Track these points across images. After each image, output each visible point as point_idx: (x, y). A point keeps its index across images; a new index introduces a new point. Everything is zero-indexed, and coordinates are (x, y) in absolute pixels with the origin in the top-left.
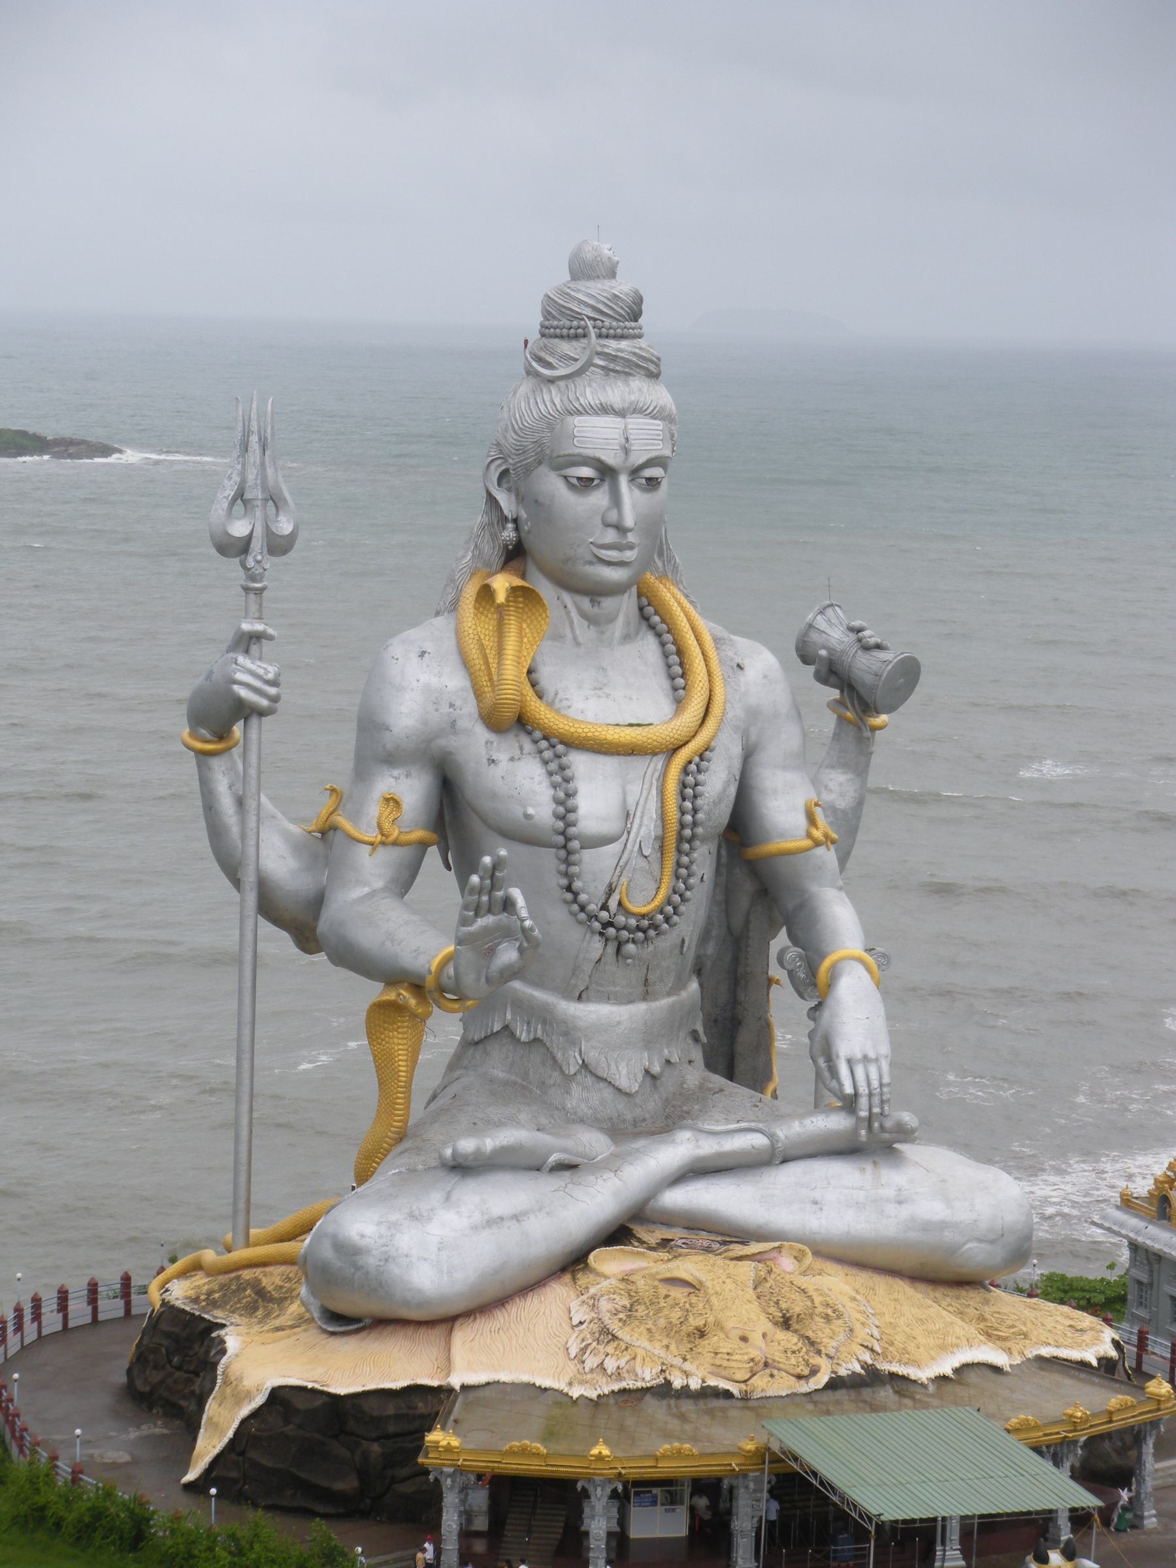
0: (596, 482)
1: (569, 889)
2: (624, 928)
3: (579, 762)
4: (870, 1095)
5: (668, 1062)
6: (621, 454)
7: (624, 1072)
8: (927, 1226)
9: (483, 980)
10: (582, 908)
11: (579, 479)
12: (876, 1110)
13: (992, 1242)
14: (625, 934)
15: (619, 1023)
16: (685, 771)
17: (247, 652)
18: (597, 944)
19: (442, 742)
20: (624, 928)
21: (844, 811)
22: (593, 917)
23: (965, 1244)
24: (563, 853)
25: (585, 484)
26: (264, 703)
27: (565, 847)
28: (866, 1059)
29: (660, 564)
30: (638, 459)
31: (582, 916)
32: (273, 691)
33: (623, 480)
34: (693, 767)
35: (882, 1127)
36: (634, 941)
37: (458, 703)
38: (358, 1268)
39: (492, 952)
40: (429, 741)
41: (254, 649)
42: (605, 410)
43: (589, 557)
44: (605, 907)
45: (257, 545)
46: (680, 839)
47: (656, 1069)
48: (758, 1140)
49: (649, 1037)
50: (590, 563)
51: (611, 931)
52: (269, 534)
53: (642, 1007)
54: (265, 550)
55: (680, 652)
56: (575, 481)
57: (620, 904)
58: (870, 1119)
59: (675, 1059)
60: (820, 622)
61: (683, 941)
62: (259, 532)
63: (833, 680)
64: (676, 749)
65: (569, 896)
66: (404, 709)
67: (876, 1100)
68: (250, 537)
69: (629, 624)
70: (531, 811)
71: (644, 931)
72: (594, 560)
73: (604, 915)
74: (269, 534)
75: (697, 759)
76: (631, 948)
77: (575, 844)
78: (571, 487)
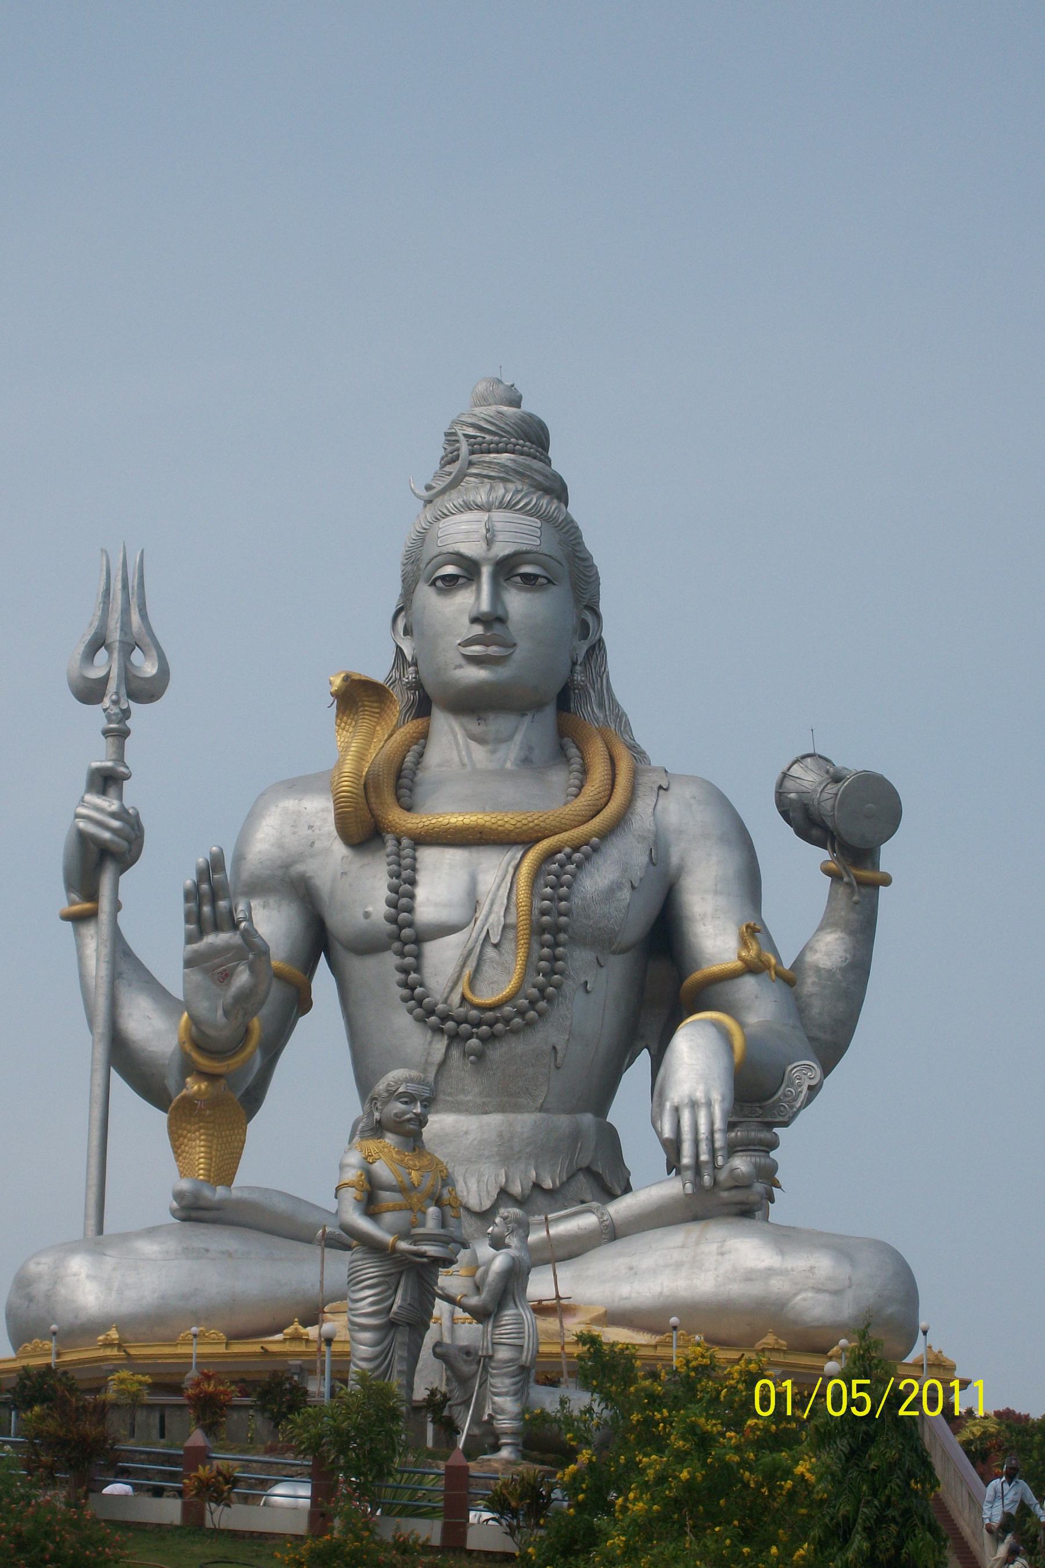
0: (461, 581)
1: (404, 985)
2: (466, 1021)
3: (428, 856)
4: (696, 1142)
5: (537, 1186)
6: (484, 546)
7: (473, 1186)
8: (749, 1276)
9: (220, 1012)
10: (420, 1003)
11: (443, 578)
12: (704, 1157)
13: (836, 1293)
14: (465, 1027)
15: (466, 1133)
16: (549, 856)
17: (103, 792)
18: (440, 1046)
19: (300, 868)
20: (466, 1021)
21: (829, 971)
22: (431, 1012)
23: (796, 1294)
24: (396, 945)
25: (450, 584)
26: (107, 835)
27: (398, 938)
28: (694, 1105)
29: (601, 716)
30: (502, 550)
31: (419, 1010)
32: (116, 824)
33: (486, 571)
34: (559, 856)
35: (715, 1182)
36: (478, 1037)
37: (318, 823)
38: (31, 1299)
39: (226, 977)
40: (286, 866)
41: (112, 791)
42: (468, 507)
43: (461, 661)
44: (445, 1001)
45: (112, 686)
46: (537, 930)
47: (516, 1189)
48: (588, 1221)
49: (507, 1152)
50: (460, 666)
51: (450, 1024)
52: (128, 675)
53: (495, 1120)
54: (123, 691)
55: (585, 771)
56: (439, 583)
57: (464, 999)
58: (697, 1167)
59: (548, 1184)
60: (796, 771)
61: (554, 1048)
62: (114, 673)
63: (815, 832)
64: (538, 840)
65: (405, 992)
66: (260, 835)
67: (704, 1147)
68: (105, 680)
69: (530, 749)
70: (370, 909)
71: (491, 1025)
72: (463, 662)
73: (441, 1006)
74: (128, 675)
75: (568, 850)
76: (474, 1042)
77: (406, 932)
78: (441, 592)
